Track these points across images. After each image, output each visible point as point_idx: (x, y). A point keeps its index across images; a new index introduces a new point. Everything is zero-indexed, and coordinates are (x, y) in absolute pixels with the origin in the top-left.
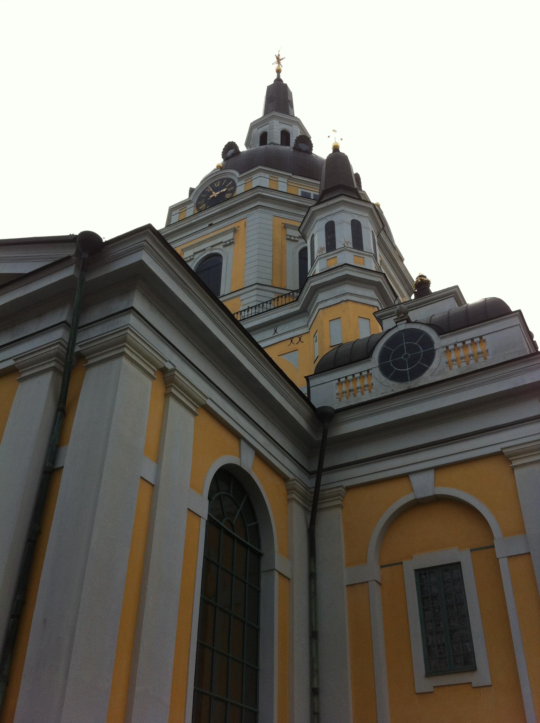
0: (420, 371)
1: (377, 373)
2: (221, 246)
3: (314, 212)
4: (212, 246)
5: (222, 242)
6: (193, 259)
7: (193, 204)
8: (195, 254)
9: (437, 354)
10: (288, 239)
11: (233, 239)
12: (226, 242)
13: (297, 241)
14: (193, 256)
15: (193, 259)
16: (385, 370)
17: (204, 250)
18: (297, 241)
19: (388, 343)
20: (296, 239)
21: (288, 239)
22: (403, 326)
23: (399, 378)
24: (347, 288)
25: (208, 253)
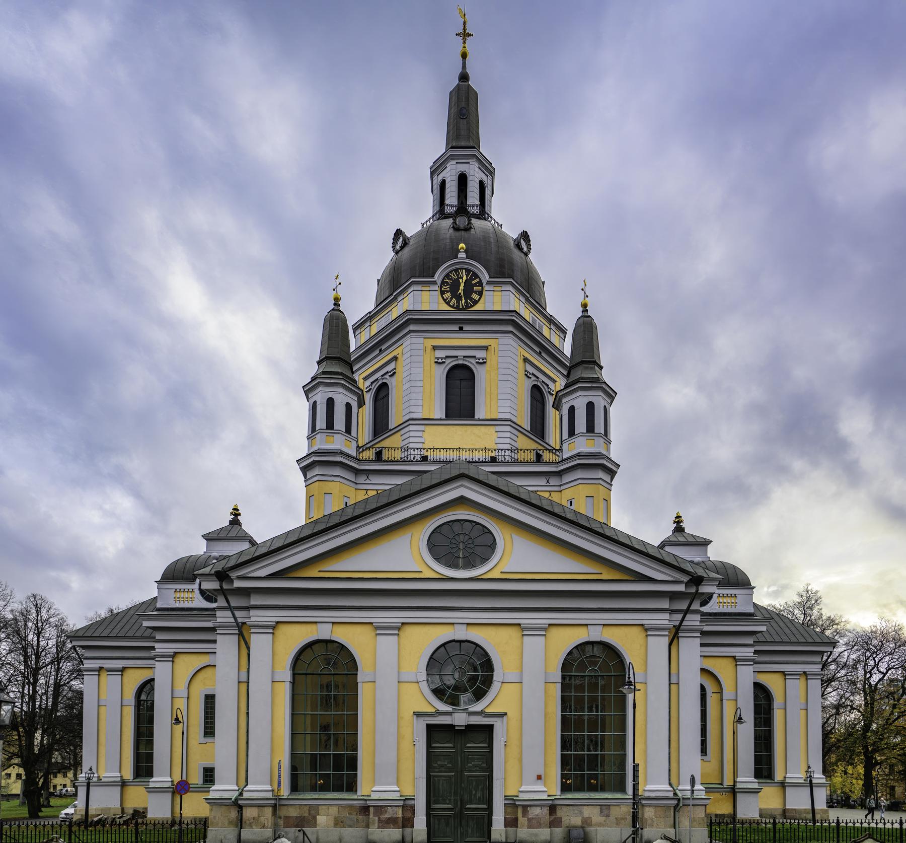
2: (387, 376)
4: (382, 376)
5: (387, 372)
6: (371, 389)
8: (372, 383)
10: (436, 362)
11: (395, 369)
12: (390, 372)
13: (444, 362)
14: (371, 385)
15: (371, 389)
17: (377, 379)
18: (444, 362)
20: (444, 360)
21: (436, 362)
25: (380, 382)
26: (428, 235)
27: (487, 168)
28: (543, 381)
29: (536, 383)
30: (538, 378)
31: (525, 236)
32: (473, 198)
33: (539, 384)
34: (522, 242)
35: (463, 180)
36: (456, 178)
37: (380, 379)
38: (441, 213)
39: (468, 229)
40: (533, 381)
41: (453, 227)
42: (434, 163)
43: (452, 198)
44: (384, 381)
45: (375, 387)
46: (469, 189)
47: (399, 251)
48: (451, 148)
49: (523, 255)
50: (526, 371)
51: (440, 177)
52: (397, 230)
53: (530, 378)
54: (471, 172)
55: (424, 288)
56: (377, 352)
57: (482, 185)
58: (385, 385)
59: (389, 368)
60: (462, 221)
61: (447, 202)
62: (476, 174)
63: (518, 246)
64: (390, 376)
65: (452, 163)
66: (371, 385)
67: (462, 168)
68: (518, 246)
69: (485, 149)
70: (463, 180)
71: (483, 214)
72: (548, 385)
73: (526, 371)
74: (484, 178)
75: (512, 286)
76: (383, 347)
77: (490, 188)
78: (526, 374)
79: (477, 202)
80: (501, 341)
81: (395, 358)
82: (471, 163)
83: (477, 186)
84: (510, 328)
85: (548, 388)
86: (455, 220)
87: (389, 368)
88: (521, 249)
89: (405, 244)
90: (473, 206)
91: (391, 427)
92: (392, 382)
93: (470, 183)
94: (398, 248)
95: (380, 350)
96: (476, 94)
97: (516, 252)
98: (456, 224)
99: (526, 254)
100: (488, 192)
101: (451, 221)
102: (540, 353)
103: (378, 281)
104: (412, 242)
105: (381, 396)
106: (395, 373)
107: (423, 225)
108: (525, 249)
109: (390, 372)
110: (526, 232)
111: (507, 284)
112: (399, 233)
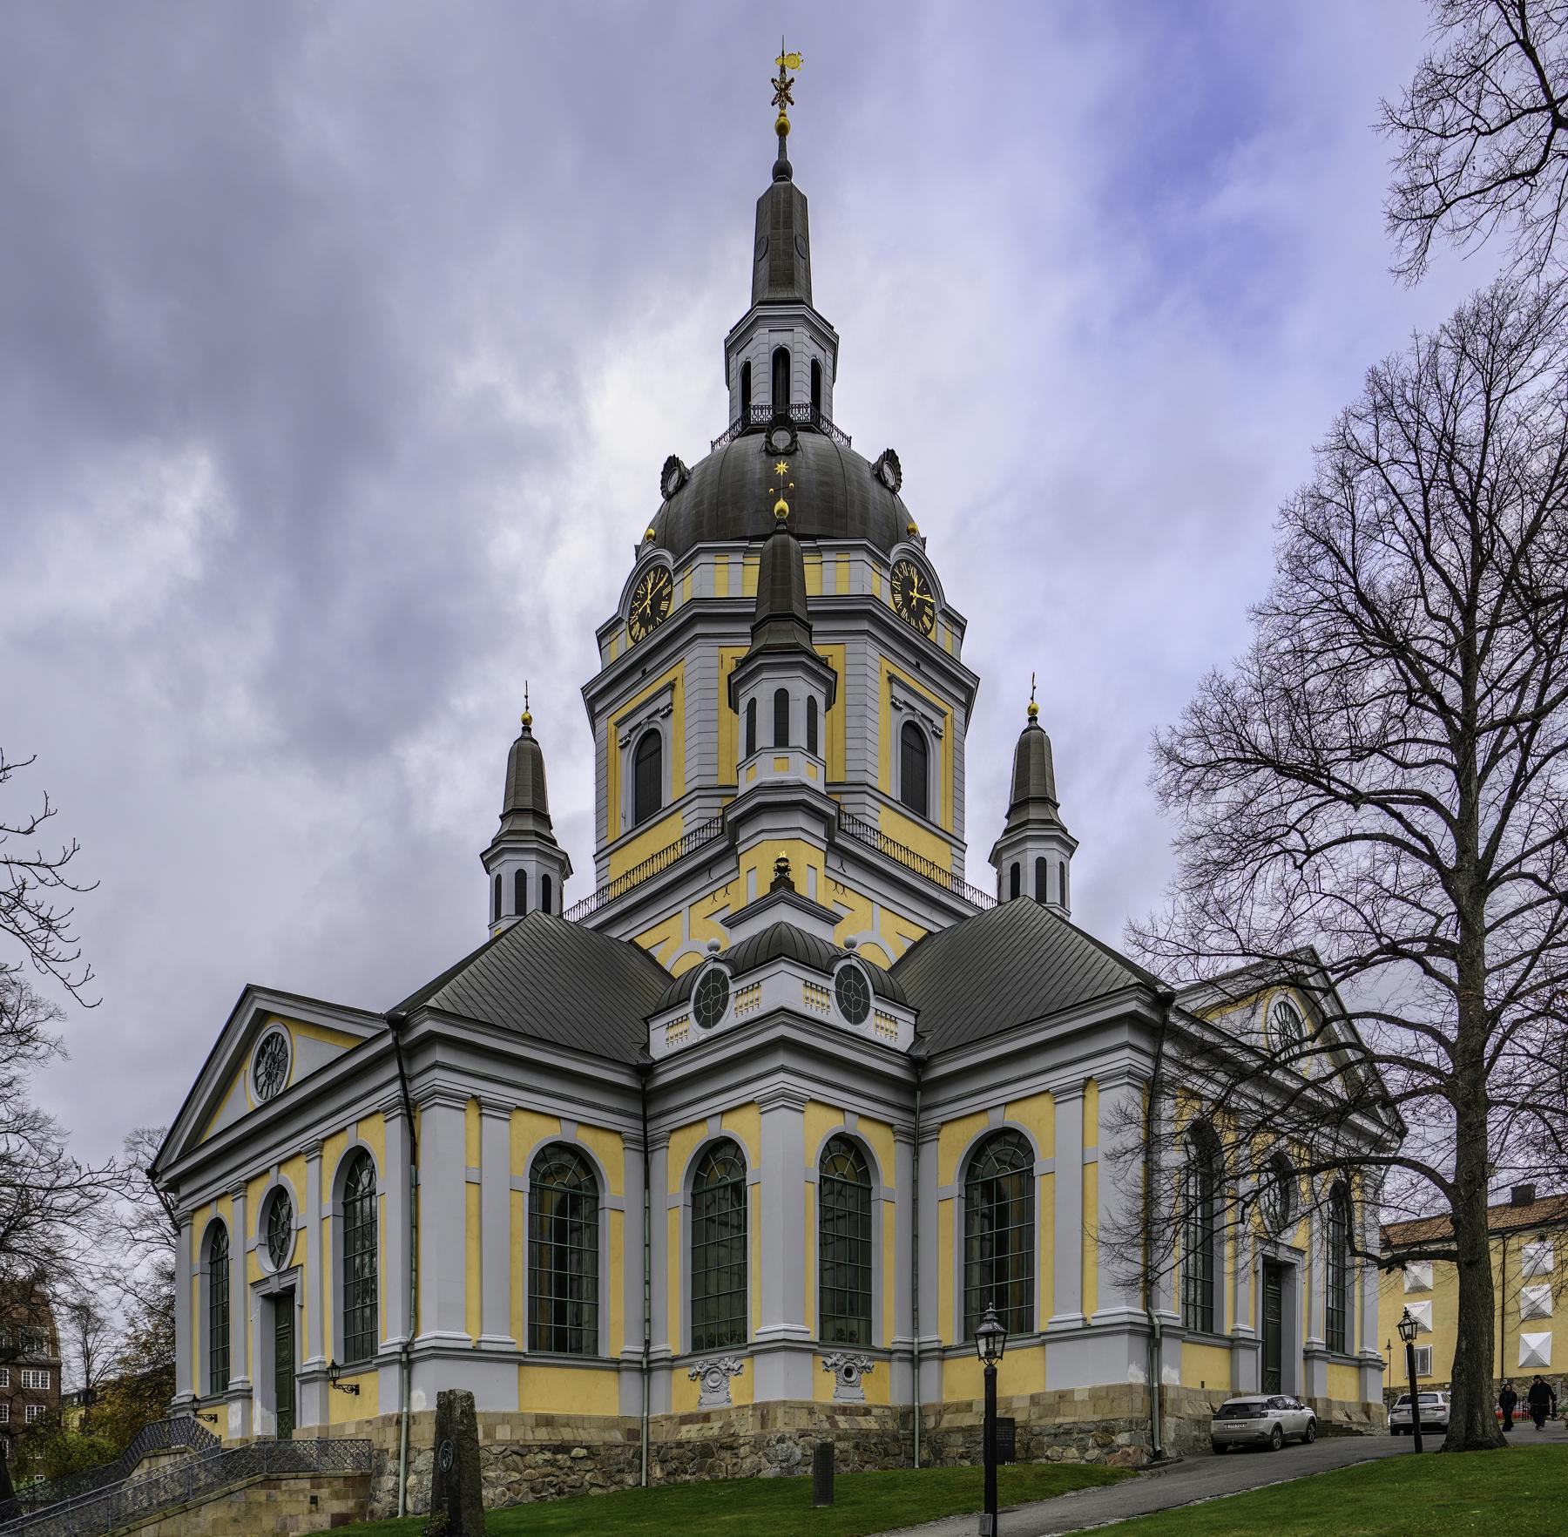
0: (718, 1017)
1: (692, 1016)
2: (657, 718)
3: (736, 683)
4: (649, 717)
5: (658, 711)
6: (629, 741)
7: (624, 626)
8: (631, 731)
9: (731, 998)
11: (671, 704)
12: (663, 710)
14: (629, 735)
15: (629, 741)
16: (697, 1012)
17: (640, 724)
19: (700, 985)
22: (710, 967)
23: (706, 1023)
24: (766, 822)
25: (646, 729)
26: (721, 465)
27: (827, 338)
28: (923, 715)
29: (911, 718)
30: (914, 709)
31: (890, 457)
32: (800, 393)
33: (917, 720)
34: (886, 469)
35: (781, 358)
36: (768, 359)
37: (645, 724)
38: (744, 425)
39: (790, 452)
40: (905, 716)
41: (766, 450)
42: (731, 332)
43: (762, 395)
44: (652, 726)
45: (635, 739)
46: (794, 377)
47: (674, 494)
48: (759, 304)
49: (887, 493)
50: (892, 697)
51: (742, 358)
52: (670, 458)
53: (901, 709)
54: (797, 347)
55: (718, 560)
56: (638, 675)
57: (816, 368)
58: (653, 735)
59: (661, 703)
60: (781, 439)
61: (753, 402)
62: (805, 350)
63: (879, 477)
64: (663, 717)
65: (761, 331)
66: (629, 735)
67: (780, 339)
68: (879, 477)
69: (823, 301)
70: (781, 358)
71: (818, 421)
72: (931, 721)
73: (892, 697)
74: (820, 355)
75: (868, 552)
76: (649, 667)
77: (829, 372)
78: (893, 704)
79: (808, 400)
80: (850, 648)
81: (671, 686)
82: (796, 329)
83: (808, 371)
84: (865, 626)
85: (933, 726)
86: (769, 437)
87: (661, 703)
88: (884, 483)
89: (683, 482)
90: (799, 407)
91: (665, 804)
92: (667, 728)
93: (794, 367)
94: (671, 489)
95: (644, 672)
96: (804, 199)
97: (875, 487)
98: (771, 445)
99: (893, 491)
100: (825, 379)
101: (762, 437)
102: (918, 665)
103: (637, 548)
104: (694, 480)
105: (645, 753)
106: (671, 711)
107: (713, 444)
108: (892, 483)
109: (663, 710)
110: (893, 451)
111: (858, 549)
112: (672, 464)
